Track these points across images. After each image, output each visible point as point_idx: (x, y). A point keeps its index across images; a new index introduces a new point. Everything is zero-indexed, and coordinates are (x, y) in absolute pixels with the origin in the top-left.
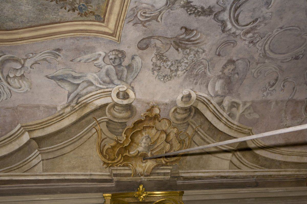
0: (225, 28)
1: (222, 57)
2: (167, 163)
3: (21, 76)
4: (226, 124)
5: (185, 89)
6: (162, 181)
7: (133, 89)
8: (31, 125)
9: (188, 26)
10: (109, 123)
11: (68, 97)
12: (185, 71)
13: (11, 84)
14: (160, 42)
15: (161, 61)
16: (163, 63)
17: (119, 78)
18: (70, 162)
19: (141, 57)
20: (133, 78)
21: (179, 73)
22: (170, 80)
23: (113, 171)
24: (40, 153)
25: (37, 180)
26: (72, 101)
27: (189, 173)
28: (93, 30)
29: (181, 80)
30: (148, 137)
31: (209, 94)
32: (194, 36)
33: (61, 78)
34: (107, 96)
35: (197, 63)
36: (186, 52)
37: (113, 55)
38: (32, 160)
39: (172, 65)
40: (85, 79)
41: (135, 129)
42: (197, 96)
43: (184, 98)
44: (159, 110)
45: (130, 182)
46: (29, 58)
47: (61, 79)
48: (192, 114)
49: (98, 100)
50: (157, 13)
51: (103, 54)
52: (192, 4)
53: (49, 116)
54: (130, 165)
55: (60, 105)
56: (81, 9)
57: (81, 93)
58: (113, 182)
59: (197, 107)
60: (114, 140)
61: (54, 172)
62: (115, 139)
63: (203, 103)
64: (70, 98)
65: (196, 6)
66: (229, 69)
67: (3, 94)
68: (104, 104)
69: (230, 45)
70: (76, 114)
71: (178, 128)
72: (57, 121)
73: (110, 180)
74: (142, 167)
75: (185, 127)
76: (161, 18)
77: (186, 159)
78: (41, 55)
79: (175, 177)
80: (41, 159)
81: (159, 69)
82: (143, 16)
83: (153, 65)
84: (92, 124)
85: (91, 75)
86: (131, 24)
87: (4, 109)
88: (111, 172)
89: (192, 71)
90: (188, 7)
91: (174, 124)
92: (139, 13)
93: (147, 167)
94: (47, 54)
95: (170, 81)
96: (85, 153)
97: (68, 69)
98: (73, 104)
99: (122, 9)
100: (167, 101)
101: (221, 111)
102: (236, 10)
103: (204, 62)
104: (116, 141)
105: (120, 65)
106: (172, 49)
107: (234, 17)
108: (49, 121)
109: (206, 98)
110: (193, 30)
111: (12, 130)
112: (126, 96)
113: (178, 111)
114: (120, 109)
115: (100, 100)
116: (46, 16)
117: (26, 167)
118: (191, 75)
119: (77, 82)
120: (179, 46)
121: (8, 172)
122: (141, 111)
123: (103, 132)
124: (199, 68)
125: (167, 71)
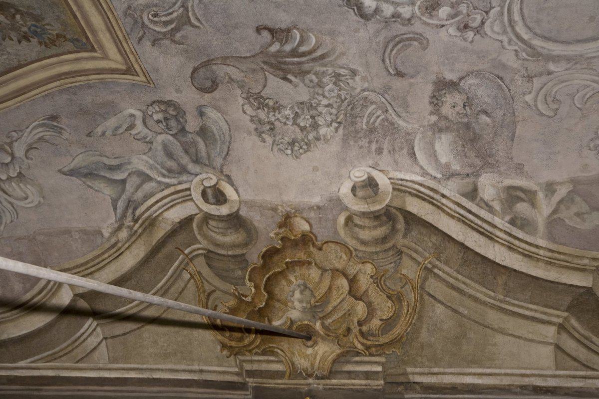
2: (368, 348)
4: (512, 246)
5: (354, 167)
6: (363, 391)
7: (229, 180)
10: (209, 256)
11: (115, 209)
13: (9, 193)
14: (234, 70)
15: (266, 109)
16: (272, 114)
17: (195, 159)
18: (155, 342)
20: (223, 157)
21: (323, 131)
23: (244, 364)
24: (98, 325)
25: (101, 378)
26: (124, 216)
27: (434, 374)
29: (335, 147)
30: (306, 287)
31: (425, 173)
33: (86, 171)
35: (353, 102)
36: (311, 81)
37: (157, 112)
38: (87, 338)
39: (297, 115)
41: (270, 269)
42: (392, 181)
43: (358, 190)
44: (308, 222)
45: (283, 390)
46: (16, 141)
53: (94, 250)
55: (105, 225)
57: (135, 198)
58: (248, 390)
60: (230, 294)
61: (131, 364)
64: (119, 211)
66: (453, 105)
67: (4, 211)
68: (186, 218)
69: (410, 45)
70: (140, 241)
71: (373, 263)
72: (111, 258)
73: (241, 383)
74: (307, 356)
75: (393, 261)
77: (419, 339)
78: (31, 132)
79: (397, 383)
80: (102, 337)
87: (15, 240)
88: (241, 367)
89: (353, 123)
91: (360, 255)
93: (318, 358)
94: (41, 129)
95: (309, 153)
97: (91, 152)
98: (128, 222)
99: (108, 18)
100: (316, 200)
103: (372, 96)
104: (236, 297)
105: (183, 130)
112: (220, 198)
114: (220, 226)
117: (79, 353)
118: (357, 132)
121: (50, 361)
123: (204, 278)
124: (368, 112)
125: (293, 131)
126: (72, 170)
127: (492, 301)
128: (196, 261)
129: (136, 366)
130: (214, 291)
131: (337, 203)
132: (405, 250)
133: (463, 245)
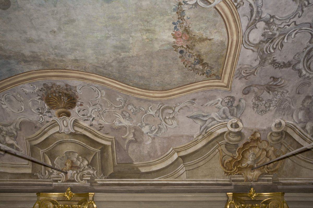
0: (300, 74)
1: (301, 94)
2: (269, 172)
3: (172, 118)
5: (277, 119)
6: (266, 185)
8: (178, 148)
9: (275, 76)
10: (227, 145)
12: (275, 106)
13: (167, 123)
15: (258, 101)
16: (259, 102)
17: (232, 114)
18: (203, 172)
19: (245, 99)
21: (271, 108)
22: (265, 113)
23: (231, 178)
25: (183, 183)
26: (203, 131)
27: (286, 180)
28: (215, 85)
29: (273, 113)
30: (254, 154)
31: (294, 121)
32: (279, 82)
34: (224, 127)
36: (275, 94)
37: (227, 100)
38: (180, 171)
39: (266, 103)
40: (210, 116)
41: (244, 148)
45: (243, 185)
46: (177, 106)
47: (195, 118)
48: (284, 136)
49: (219, 130)
50: (254, 70)
51: (221, 100)
52: (276, 61)
53: (189, 142)
54: (243, 174)
55: (195, 134)
56: (207, 73)
58: (232, 186)
59: (287, 131)
60: (230, 156)
62: (232, 156)
63: (291, 128)
64: (202, 130)
65: (279, 62)
68: (223, 132)
69: (306, 85)
73: (230, 184)
74: (251, 175)
76: (257, 73)
77: (283, 169)
79: (276, 183)
81: (258, 107)
82: (245, 73)
83: (253, 104)
84: (216, 146)
85: (214, 114)
86: (238, 78)
88: (230, 179)
90: (274, 64)
91: (271, 144)
92: (243, 71)
93: (255, 175)
94: (188, 103)
95: (265, 114)
96: (212, 166)
97: (200, 111)
98: (203, 133)
99: (232, 70)
100: (265, 128)
101: (305, 134)
102: (308, 61)
103: (289, 99)
104: (232, 157)
105: (232, 106)
106: (265, 92)
107: (307, 66)
108: (189, 145)
109: (292, 124)
110: (278, 78)
111: (167, 151)
112: (237, 126)
113: (273, 134)
115: (220, 130)
116: (188, 79)
117: (176, 175)
118: (280, 109)
119: (205, 119)
120: (270, 90)
121: (166, 178)
122: (248, 136)
126: (191, 116)
127: (303, 159)
128: (221, 146)
129: (195, 179)
130: (225, 155)
131: (270, 129)
132: (283, 143)
133: (298, 142)
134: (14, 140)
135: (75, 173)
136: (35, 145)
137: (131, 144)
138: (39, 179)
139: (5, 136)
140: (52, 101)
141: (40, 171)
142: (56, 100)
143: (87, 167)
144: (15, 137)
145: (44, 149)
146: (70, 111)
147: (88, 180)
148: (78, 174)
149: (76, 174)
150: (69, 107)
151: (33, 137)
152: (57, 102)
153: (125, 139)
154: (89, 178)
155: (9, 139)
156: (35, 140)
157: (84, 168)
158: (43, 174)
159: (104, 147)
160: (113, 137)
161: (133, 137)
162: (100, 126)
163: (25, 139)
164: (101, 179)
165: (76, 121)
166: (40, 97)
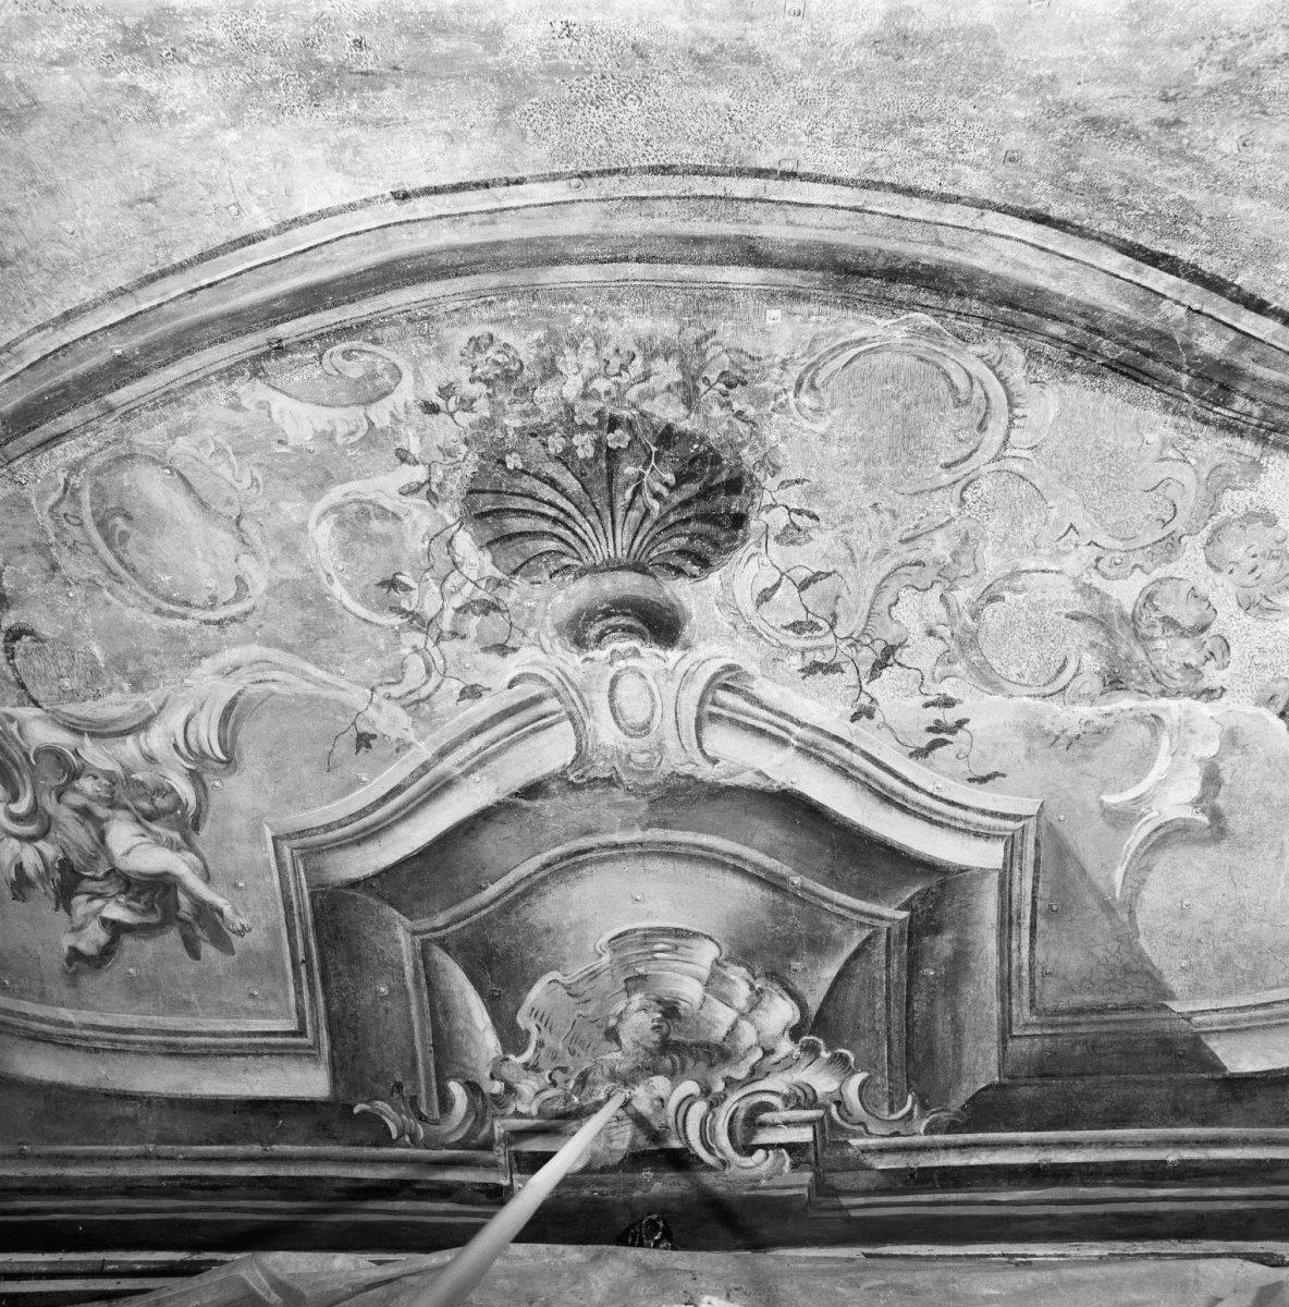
134: (172, 845)
135: (689, 1100)
136: (354, 884)
137: (1164, 859)
138: (392, 1143)
139: (101, 811)
140: (528, 504)
141: (399, 1087)
142: (563, 492)
143: (786, 1047)
144: (186, 825)
145: (431, 914)
146: (683, 592)
147: (792, 1148)
148: (715, 1103)
149: (700, 1108)
150: (676, 561)
151: (340, 824)
152: (575, 513)
153: (1120, 819)
154: (805, 1135)
155: (138, 840)
156: (358, 843)
157: (768, 1052)
158: (430, 1108)
159: (942, 885)
160: (1029, 807)
161: (1197, 802)
162: (935, 714)
163: (269, 834)
164: (897, 1134)
165: (729, 679)
166: (418, 474)
